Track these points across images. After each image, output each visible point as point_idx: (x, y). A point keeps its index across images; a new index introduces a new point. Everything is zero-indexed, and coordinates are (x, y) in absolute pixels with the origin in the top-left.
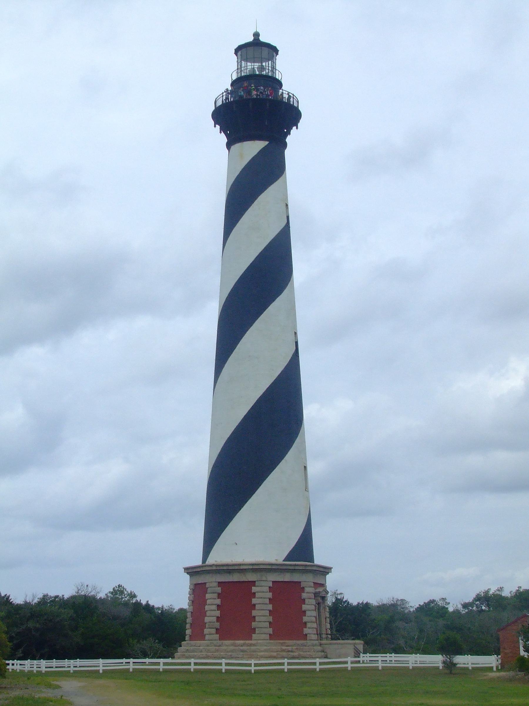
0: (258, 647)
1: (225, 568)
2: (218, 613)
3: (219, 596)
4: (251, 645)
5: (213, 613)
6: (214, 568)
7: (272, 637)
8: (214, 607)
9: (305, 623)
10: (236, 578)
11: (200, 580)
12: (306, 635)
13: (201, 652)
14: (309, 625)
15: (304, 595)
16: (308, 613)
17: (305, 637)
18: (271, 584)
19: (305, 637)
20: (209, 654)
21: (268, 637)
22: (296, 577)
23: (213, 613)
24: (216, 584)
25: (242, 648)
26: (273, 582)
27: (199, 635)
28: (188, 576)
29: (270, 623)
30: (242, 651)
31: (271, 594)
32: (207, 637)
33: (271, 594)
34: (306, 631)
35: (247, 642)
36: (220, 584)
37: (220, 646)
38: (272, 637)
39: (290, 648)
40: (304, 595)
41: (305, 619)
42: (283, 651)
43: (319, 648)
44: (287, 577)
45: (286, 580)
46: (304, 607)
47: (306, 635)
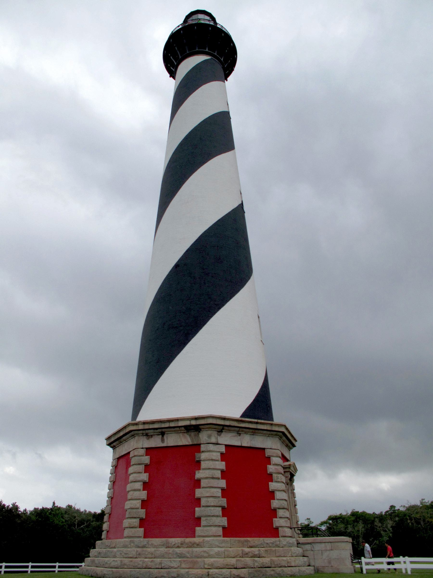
0: (205, 549)
1: (156, 426)
2: (144, 495)
3: (147, 468)
4: (193, 545)
5: (136, 494)
6: (141, 427)
7: (227, 532)
8: (139, 486)
9: (275, 510)
10: (173, 440)
11: (123, 450)
12: (277, 529)
13: (115, 557)
14: (280, 513)
15: (271, 468)
16: (278, 495)
17: (275, 532)
18: (223, 449)
19: (275, 532)
20: (126, 561)
21: (220, 531)
22: (258, 442)
23: (136, 494)
24: (143, 452)
25: (178, 550)
26: (226, 446)
27: (118, 531)
28: (111, 450)
29: (223, 508)
30: (180, 556)
31: (224, 463)
32: (126, 532)
33: (224, 463)
34: (277, 522)
35: (188, 540)
36: (149, 451)
37: (144, 547)
38: (227, 532)
39: (255, 550)
40: (271, 468)
41: (274, 504)
42: (245, 555)
43: (299, 550)
44: (246, 441)
45: (245, 444)
46: (272, 486)
47: (277, 529)
